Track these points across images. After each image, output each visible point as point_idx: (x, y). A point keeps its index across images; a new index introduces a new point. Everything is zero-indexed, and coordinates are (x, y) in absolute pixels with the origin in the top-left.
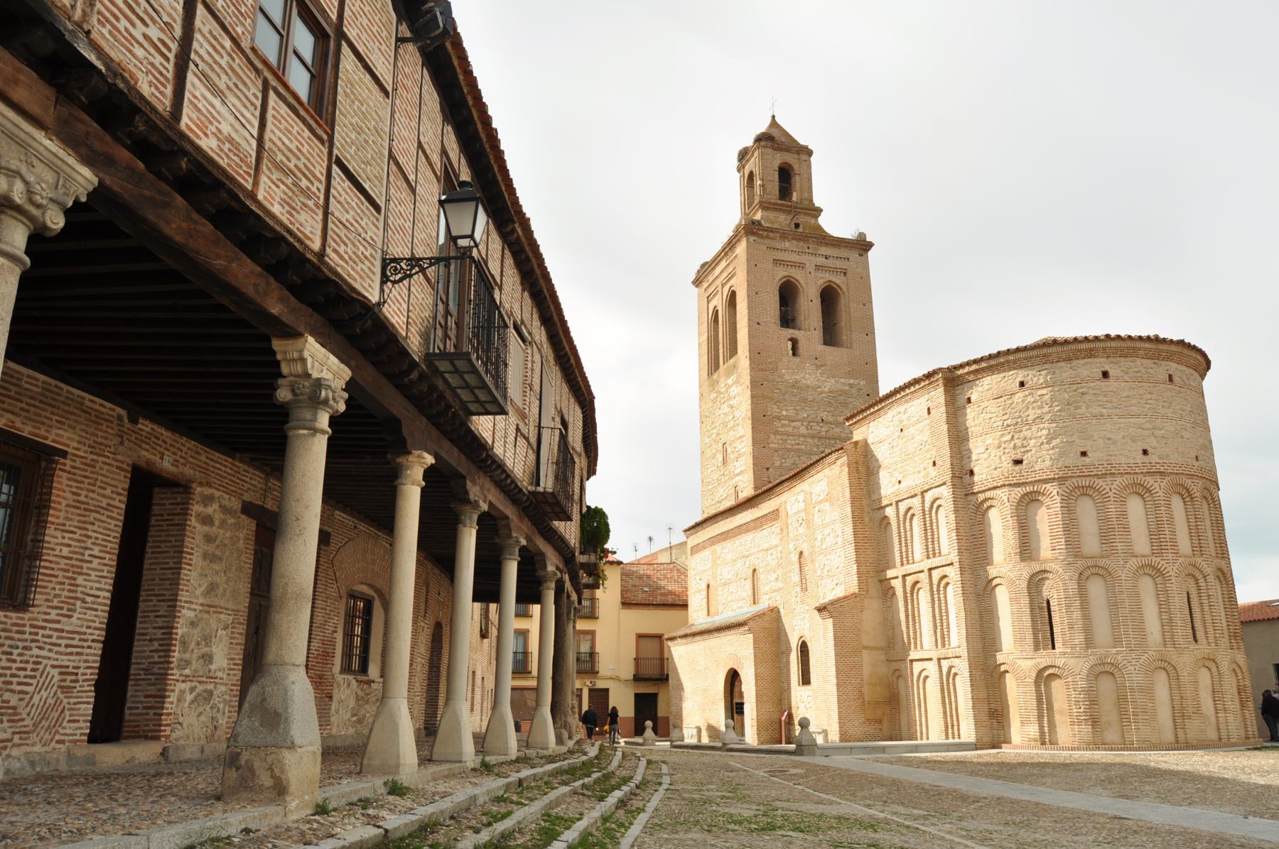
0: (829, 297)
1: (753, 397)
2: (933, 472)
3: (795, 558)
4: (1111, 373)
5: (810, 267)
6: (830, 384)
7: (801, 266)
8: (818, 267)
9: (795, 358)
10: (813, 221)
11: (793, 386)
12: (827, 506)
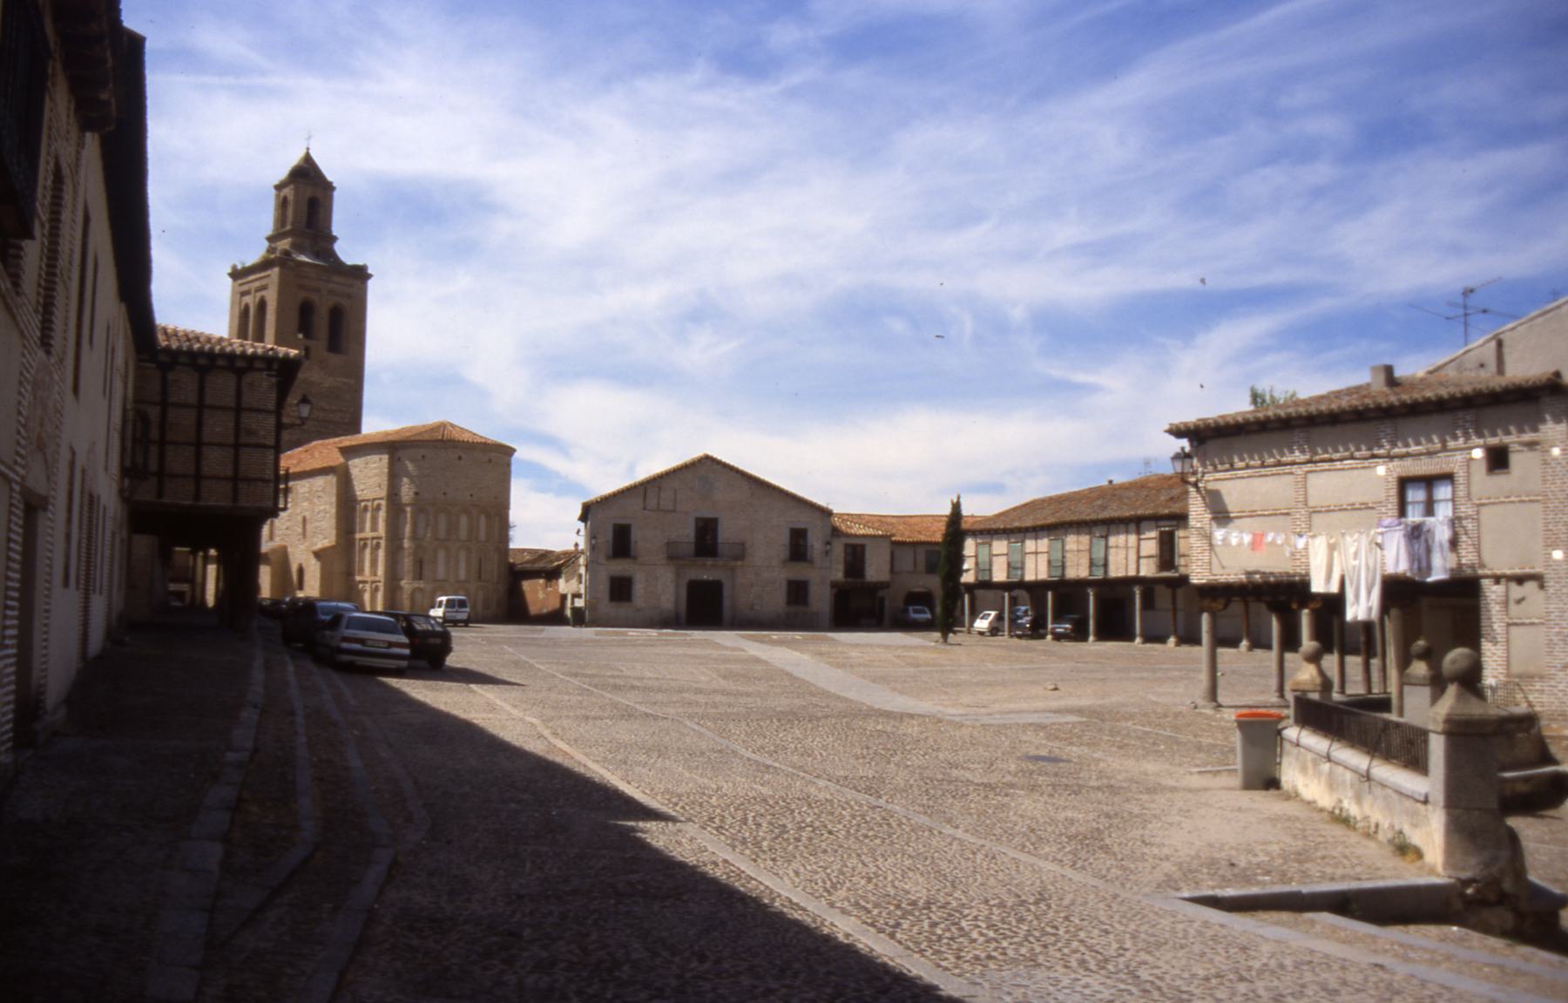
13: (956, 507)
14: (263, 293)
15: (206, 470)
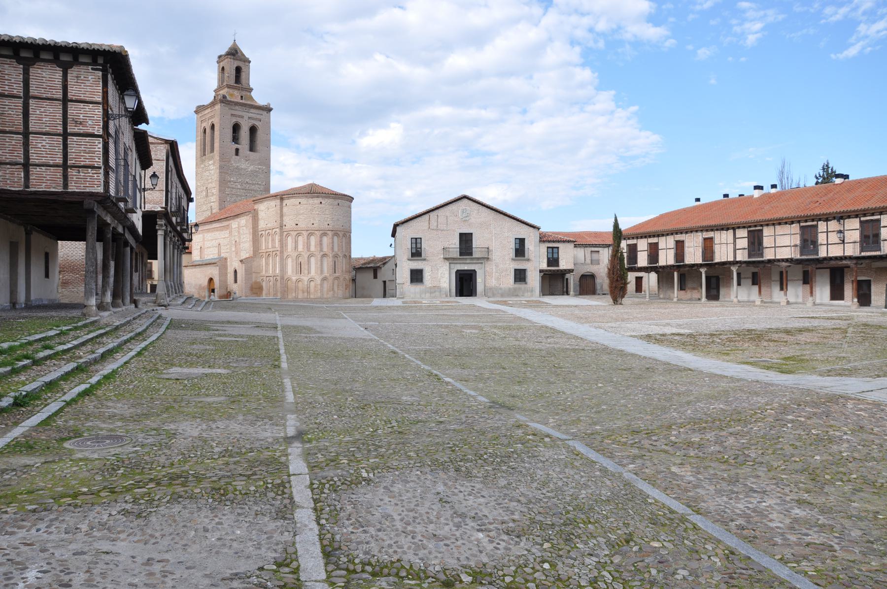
0: (253, 130)
1: (220, 172)
2: (275, 224)
3: (234, 242)
4: (323, 202)
5: (246, 118)
6: (251, 168)
7: (242, 117)
8: (249, 118)
9: (236, 157)
10: (249, 94)
11: (236, 169)
12: (245, 228)
13: (616, 225)
14: (213, 120)
15: (34, 158)
